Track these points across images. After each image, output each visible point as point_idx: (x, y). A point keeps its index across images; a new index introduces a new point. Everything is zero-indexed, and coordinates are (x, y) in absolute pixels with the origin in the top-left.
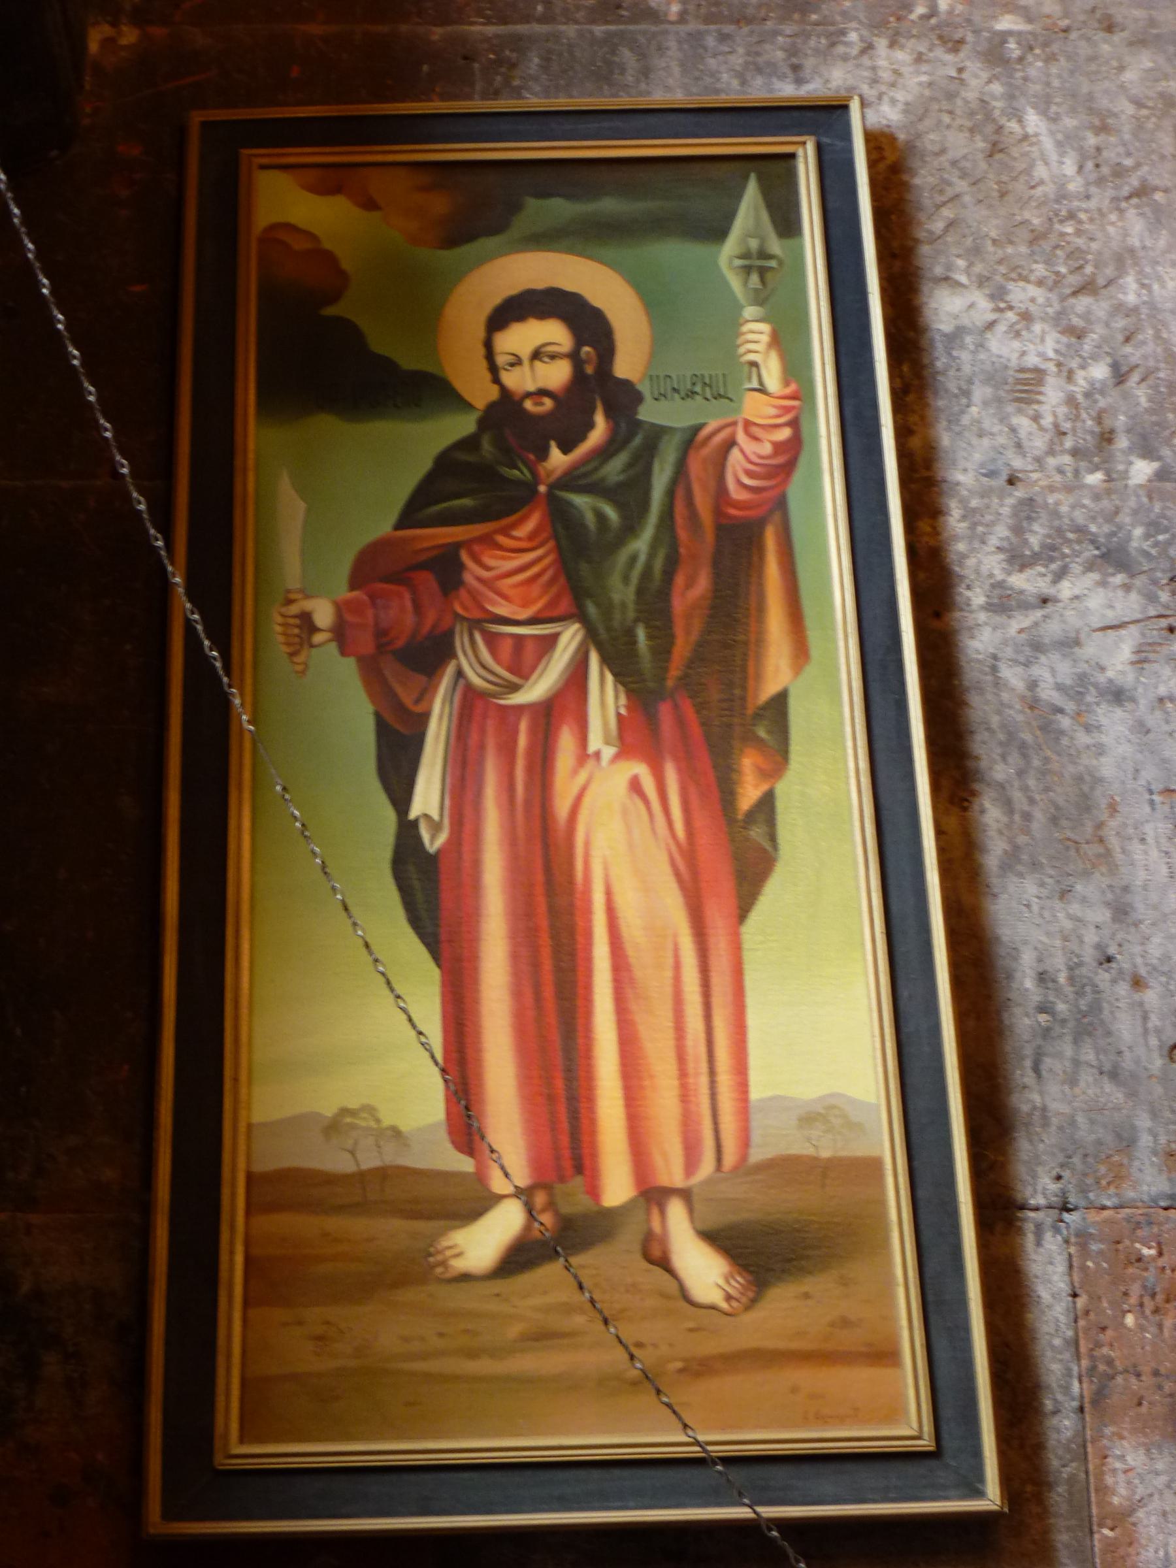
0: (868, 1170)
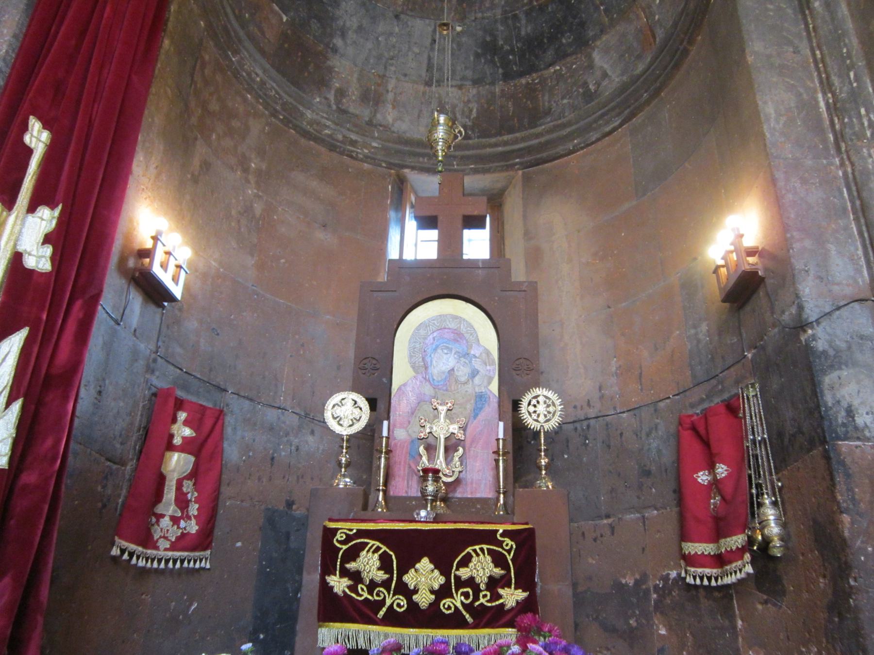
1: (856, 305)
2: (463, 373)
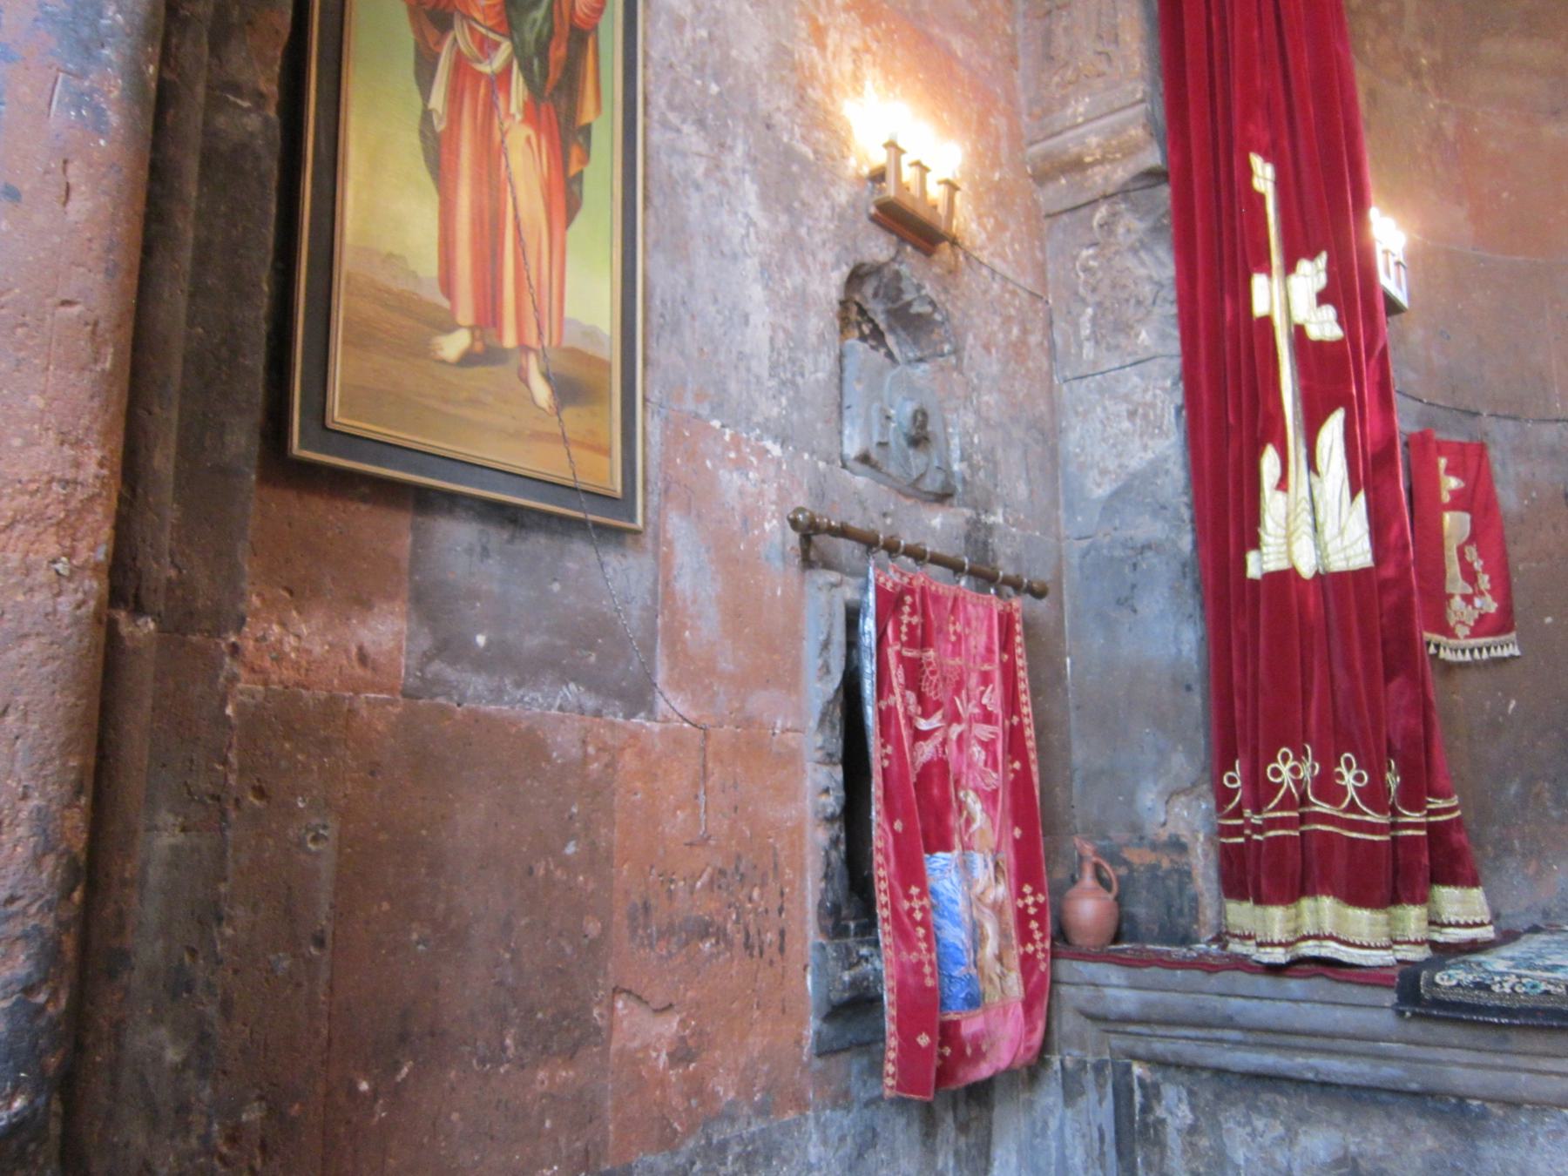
0: (606, 366)
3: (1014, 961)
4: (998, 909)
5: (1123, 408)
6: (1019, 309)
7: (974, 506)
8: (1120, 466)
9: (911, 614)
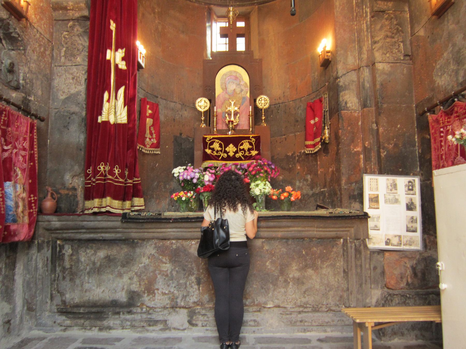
1: (353, 72)
2: (238, 90)
3: (26, 213)
4: (23, 199)
5: (71, 76)
6: (44, 43)
7: (26, 94)
8: (68, 91)
9: (5, 117)
